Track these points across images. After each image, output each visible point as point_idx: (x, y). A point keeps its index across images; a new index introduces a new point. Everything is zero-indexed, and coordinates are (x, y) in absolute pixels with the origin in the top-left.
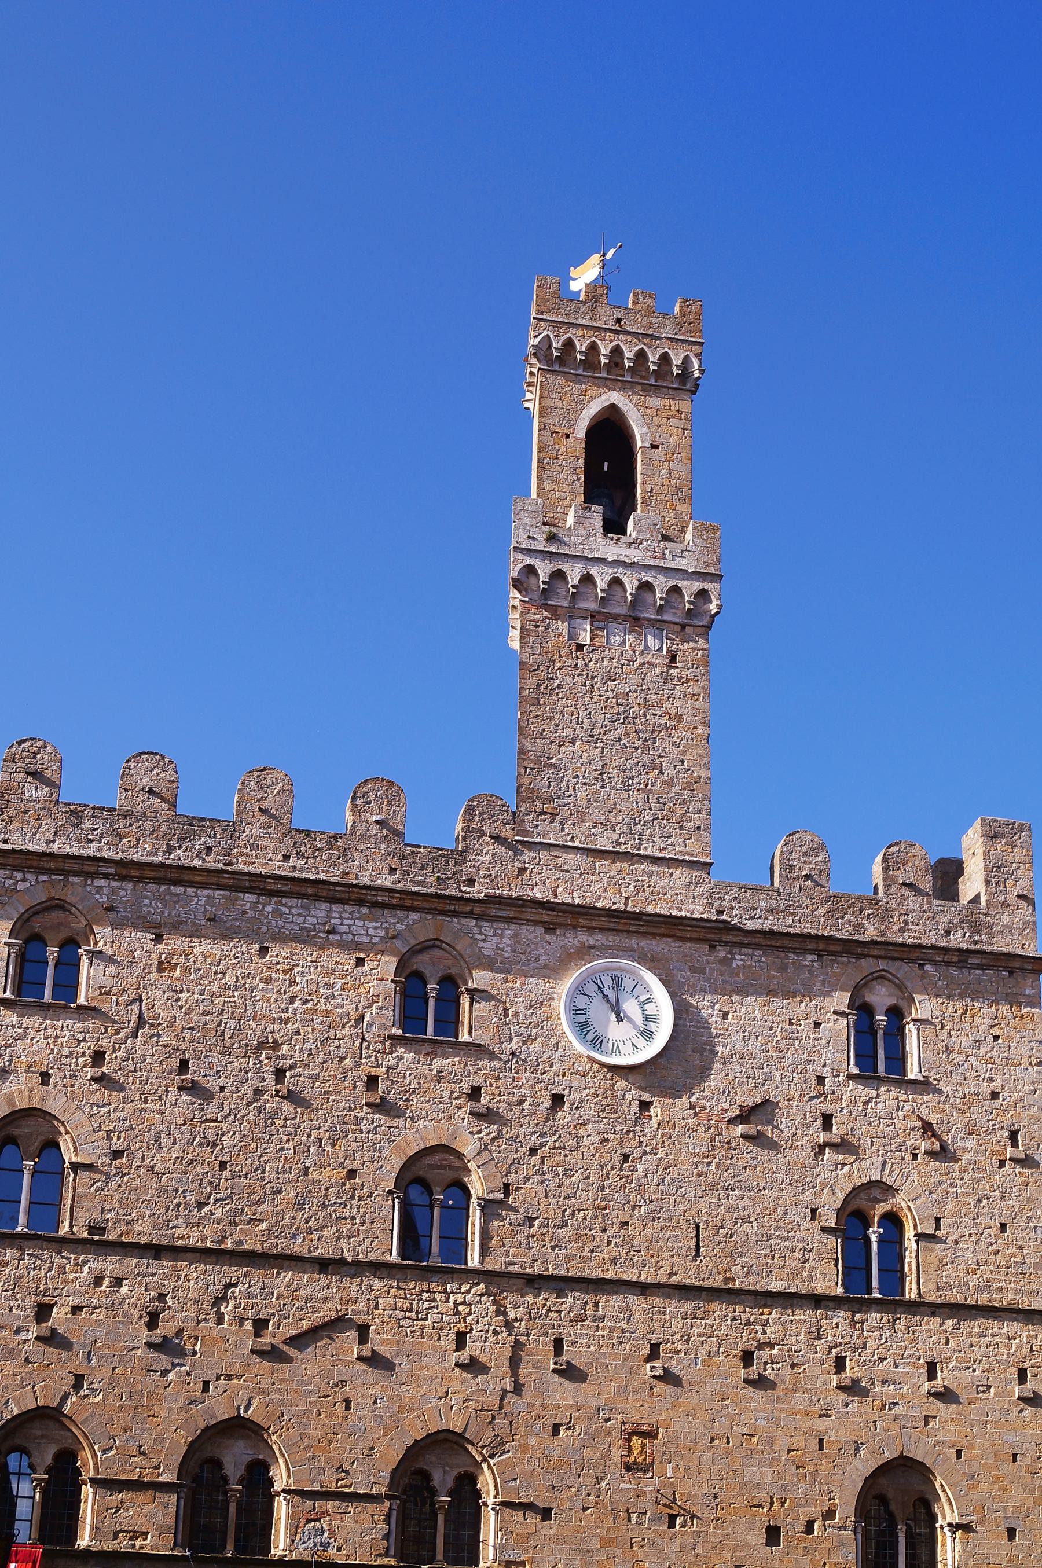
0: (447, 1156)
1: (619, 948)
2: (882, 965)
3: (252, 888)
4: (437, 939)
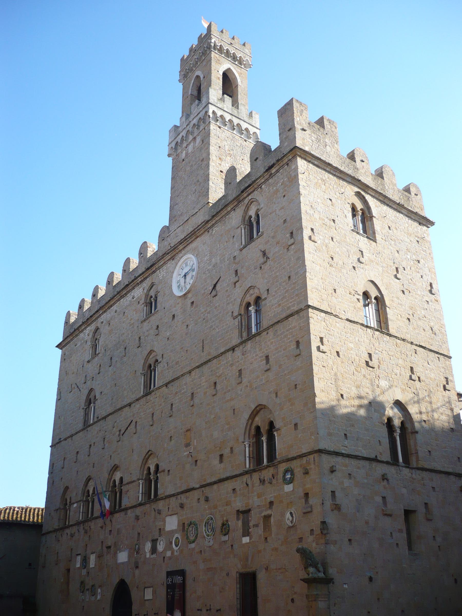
2: (250, 197)
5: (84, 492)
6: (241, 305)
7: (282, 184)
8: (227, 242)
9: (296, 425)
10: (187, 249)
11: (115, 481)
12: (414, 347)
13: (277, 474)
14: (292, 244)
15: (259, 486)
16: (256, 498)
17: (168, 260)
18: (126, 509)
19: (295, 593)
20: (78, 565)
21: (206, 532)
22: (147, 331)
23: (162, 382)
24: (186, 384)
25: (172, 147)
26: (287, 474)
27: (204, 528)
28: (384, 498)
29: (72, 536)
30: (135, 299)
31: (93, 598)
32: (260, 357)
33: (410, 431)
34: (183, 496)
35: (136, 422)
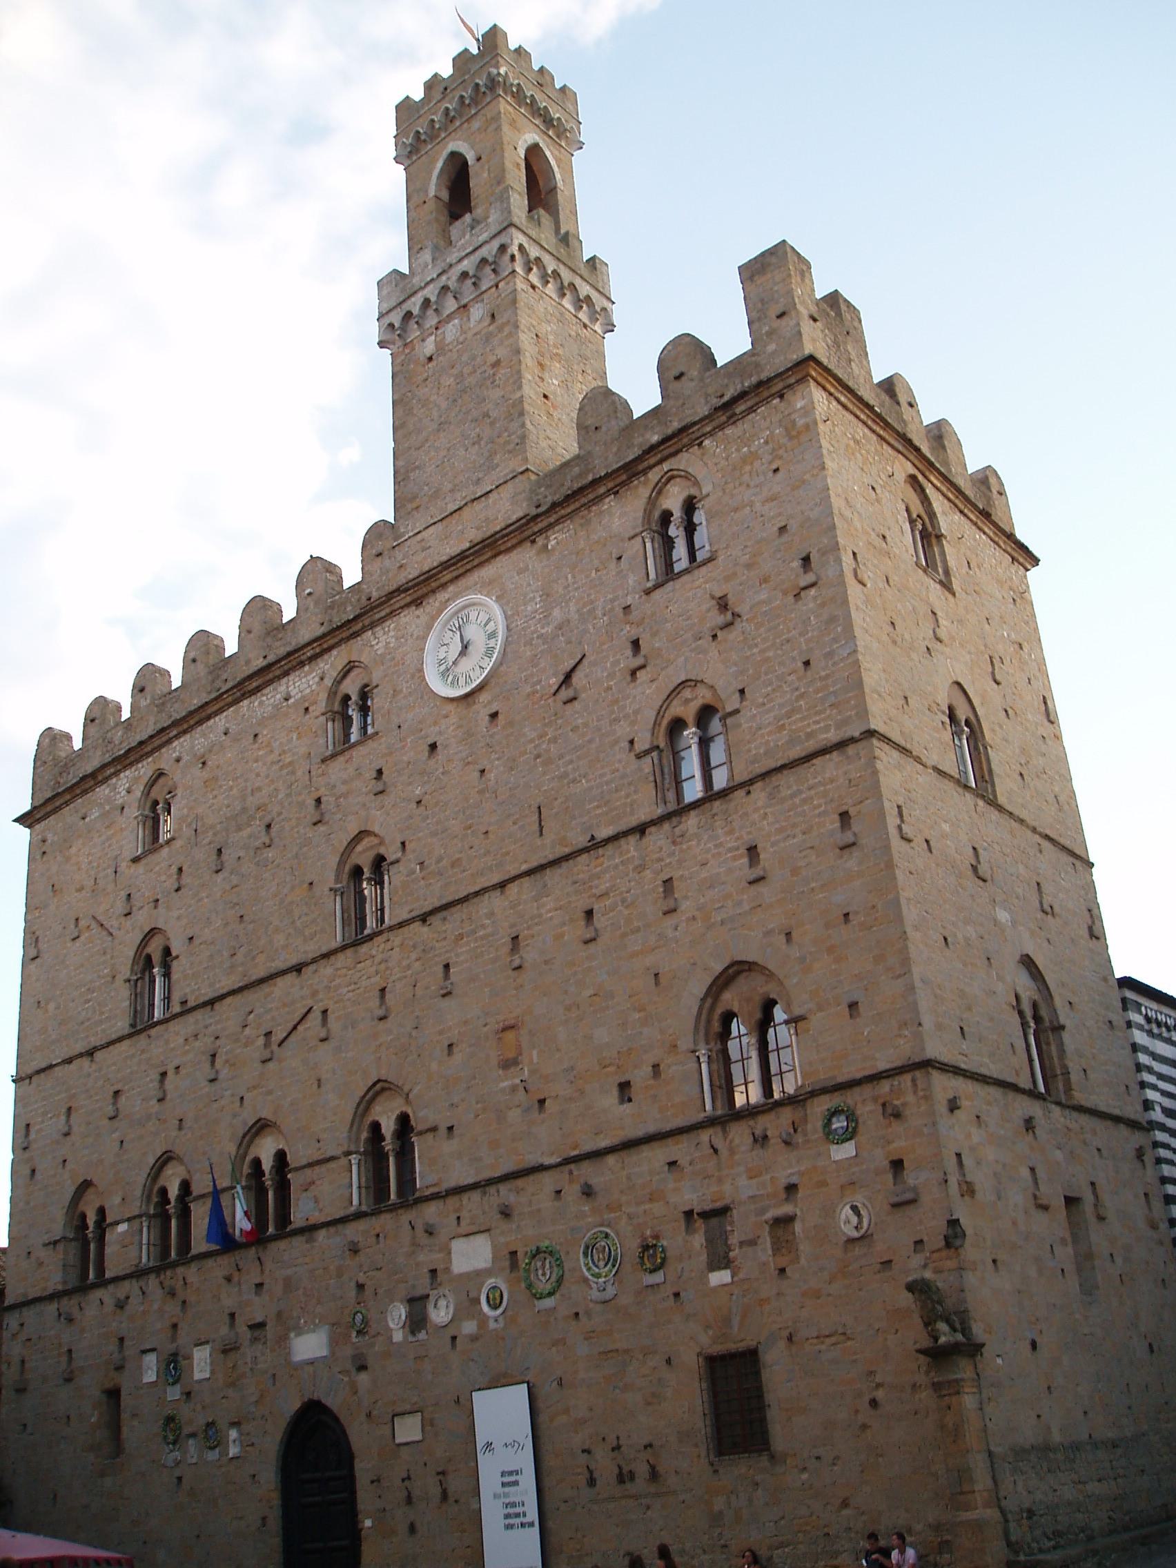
1: (468, 588)
2: (666, 466)
5: (151, 1190)
6: (656, 724)
7: (766, 442)
8: (597, 570)
9: (853, 1006)
10: (462, 583)
11: (257, 1163)
12: (1037, 838)
13: (805, 1120)
14: (813, 585)
16: (743, 1181)
17: (402, 608)
18: (310, 1229)
19: (878, 1386)
20: (150, 1376)
21: (589, 1269)
22: (345, 782)
23: (407, 909)
24: (491, 914)
25: (391, 326)
26: (834, 1120)
28: (1032, 1169)
29: (121, 1305)
30: (291, 701)
31: (212, 1456)
32: (730, 850)
33: (1047, 1024)
34: (503, 1188)
35: (325, 1012)
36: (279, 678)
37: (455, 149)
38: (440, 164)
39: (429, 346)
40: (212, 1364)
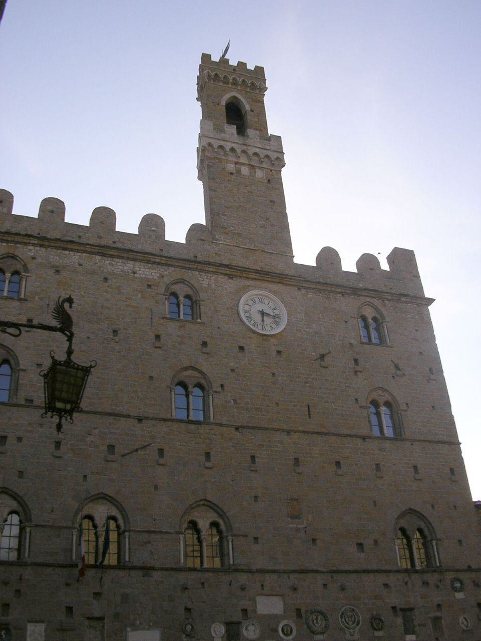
0: (193, 372)
1: (261, 287)
2: (368, 299)
3: (99, 253)
4: (182, 279)
7: (412, 318)
9: (460, 541)
15: (422, 587)
17: (221, 273)
18: (147, 570)
21: (344, 625)
25: (210, 145)
26: (455, 583)
27: (340, 620)
36: (128, 259)
37: (236, 96)
38: (227, 97)
39: (231, 167)
40: (45, 636)
